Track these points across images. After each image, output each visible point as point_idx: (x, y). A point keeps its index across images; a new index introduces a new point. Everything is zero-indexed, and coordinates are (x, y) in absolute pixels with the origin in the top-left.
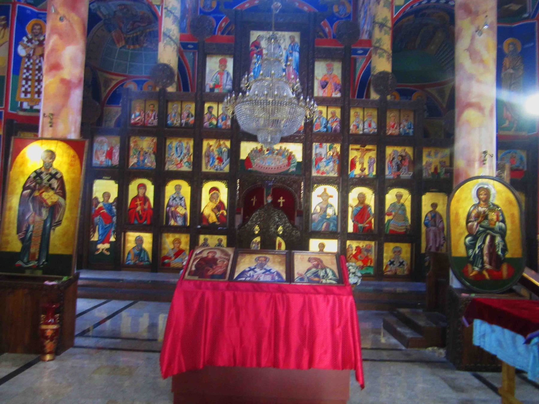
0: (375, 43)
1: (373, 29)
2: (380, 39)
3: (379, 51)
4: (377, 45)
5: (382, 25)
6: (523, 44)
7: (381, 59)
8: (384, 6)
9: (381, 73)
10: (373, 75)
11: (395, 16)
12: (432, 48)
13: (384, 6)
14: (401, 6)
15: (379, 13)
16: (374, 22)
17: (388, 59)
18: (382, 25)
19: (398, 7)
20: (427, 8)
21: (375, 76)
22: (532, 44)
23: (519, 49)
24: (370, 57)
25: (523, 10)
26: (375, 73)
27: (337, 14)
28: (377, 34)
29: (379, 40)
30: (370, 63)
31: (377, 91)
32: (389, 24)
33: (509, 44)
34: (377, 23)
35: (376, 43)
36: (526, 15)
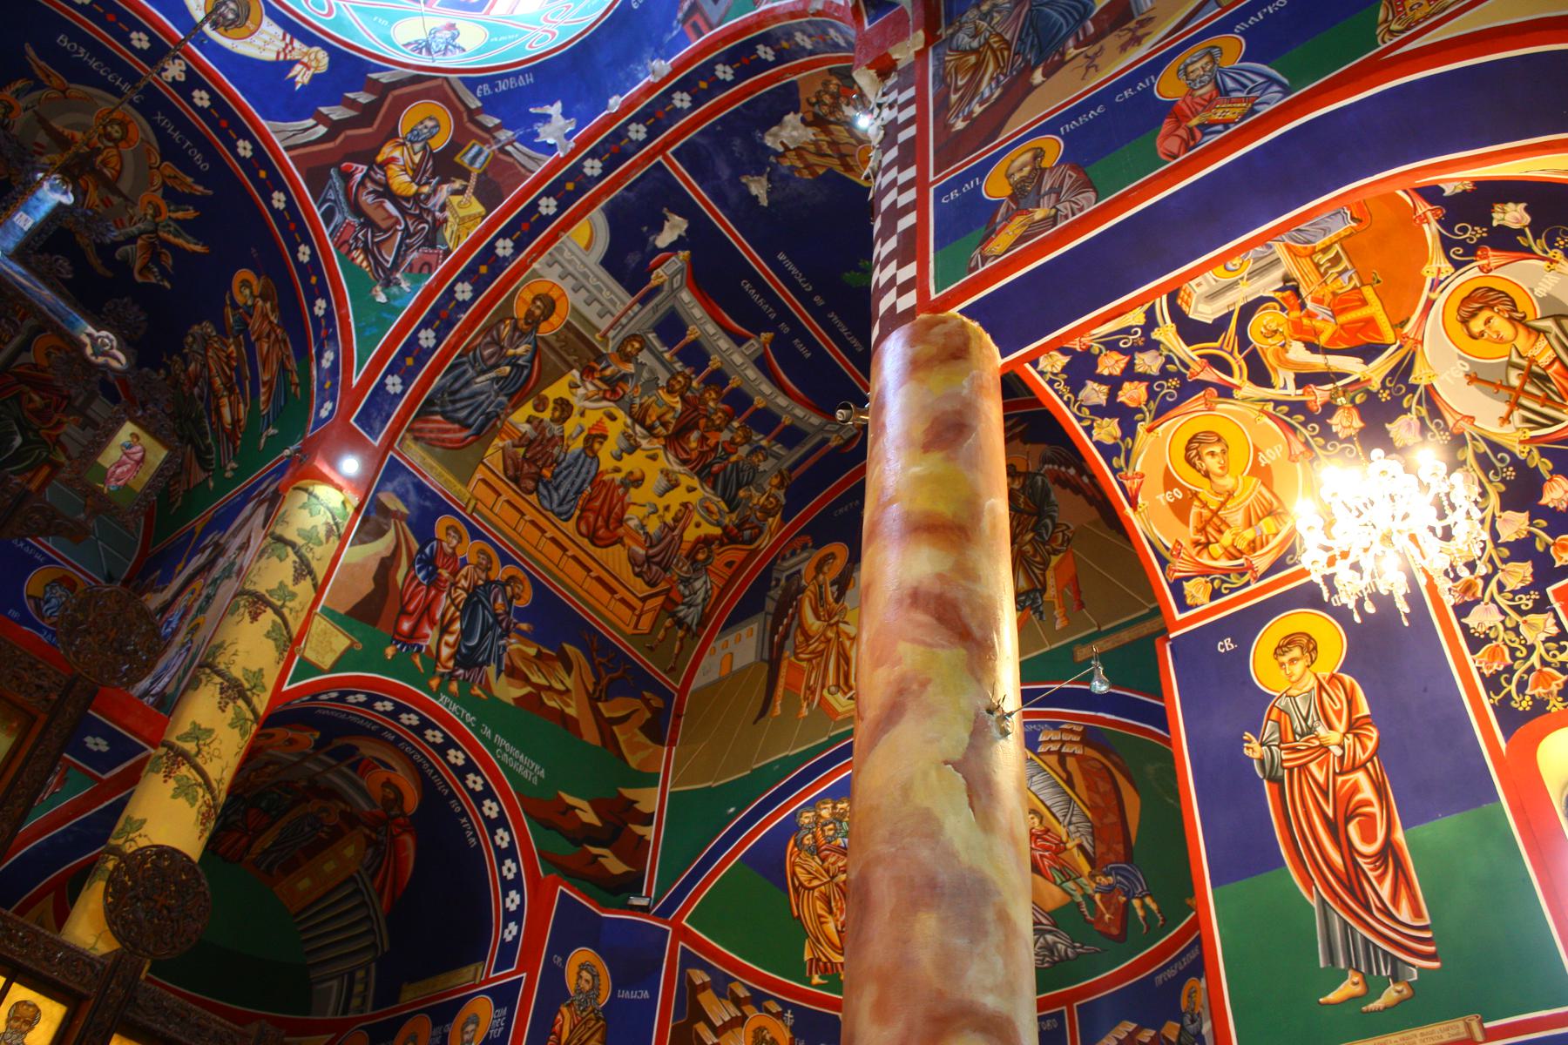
0: (185, 737)
1: (194, 684)
2: (210, 731)
3: (185, 770)
4: (190, 747)
5: (234, 690)
6: (617, 984)
7: (182, 801)
8: (268, 635)
9: (162, 851)
10: (116, 851)
11: (286, 688)
12: (305, 884)
13: (268, 635)
14: (313, 669)
15: (241, 647)
16: (209, 665)
17: (205, 818)
18: (234, 690)
19: (308, 668)
20: (377, 734)
21: (124, 857)
22: (646, 994)
23: (604, 997)
24: (132, 779)
25: (632, 884)
26: (129, 848)
27: (30, 605)
28: (203, 706)
29: (199, 733)
30: (131, 794)
31: (115, 916)
32: (262, 702)
33: (583, 967)
34: (220, 674)
35: (185, 737)
36: (635, 901)
